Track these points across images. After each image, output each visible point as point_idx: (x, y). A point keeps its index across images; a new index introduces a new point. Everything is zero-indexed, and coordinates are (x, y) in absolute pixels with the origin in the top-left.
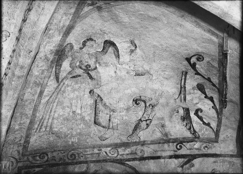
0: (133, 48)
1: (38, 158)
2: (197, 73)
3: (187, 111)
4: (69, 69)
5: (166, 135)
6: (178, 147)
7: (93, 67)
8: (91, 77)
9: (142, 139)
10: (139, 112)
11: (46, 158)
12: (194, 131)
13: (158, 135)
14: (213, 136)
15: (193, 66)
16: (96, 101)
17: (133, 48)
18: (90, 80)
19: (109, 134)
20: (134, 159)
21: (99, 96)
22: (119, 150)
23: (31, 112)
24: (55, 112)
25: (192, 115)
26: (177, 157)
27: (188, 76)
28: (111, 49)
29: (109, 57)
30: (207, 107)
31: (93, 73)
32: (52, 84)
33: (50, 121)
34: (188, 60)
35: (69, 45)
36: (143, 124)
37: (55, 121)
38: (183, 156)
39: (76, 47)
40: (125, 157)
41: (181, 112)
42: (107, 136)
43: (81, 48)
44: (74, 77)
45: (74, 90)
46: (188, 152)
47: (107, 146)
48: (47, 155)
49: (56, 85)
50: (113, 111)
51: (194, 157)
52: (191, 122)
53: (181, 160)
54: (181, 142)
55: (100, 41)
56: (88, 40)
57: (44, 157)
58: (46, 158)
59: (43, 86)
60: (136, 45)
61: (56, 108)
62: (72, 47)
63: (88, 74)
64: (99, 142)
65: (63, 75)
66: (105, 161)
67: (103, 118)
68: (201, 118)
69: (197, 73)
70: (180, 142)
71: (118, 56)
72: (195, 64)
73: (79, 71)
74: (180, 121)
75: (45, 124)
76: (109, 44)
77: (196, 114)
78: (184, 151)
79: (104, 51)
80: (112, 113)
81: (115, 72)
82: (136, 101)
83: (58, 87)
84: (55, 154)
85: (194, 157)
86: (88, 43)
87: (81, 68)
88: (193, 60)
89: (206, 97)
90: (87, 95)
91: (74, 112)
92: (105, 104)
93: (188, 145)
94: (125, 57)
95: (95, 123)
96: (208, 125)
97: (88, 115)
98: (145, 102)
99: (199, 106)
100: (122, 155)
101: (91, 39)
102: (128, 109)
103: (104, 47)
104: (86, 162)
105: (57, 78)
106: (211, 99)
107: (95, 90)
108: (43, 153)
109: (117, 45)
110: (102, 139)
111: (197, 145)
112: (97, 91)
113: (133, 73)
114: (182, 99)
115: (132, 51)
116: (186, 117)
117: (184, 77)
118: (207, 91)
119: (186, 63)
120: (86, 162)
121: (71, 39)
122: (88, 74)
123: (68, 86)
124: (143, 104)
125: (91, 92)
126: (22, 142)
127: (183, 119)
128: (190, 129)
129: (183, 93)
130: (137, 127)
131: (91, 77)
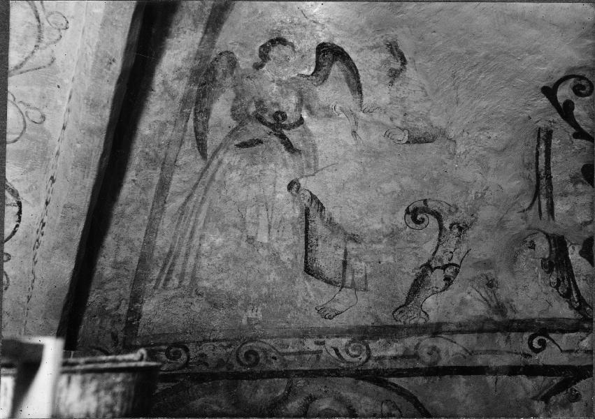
0: (397, 66)
1: (163, 356)
3: (559, 244)
5: (500, 309)
6: (535, 344)
7: (292, 117)
8: (289, 147)
9: (433, 318)
10: (427, 242)
11: (184, 356)
12: (581, 299)
13: (477, 308)
16: (307, 213)
17: (397, 66)
18: (287, 154)
19: (344, 300)
21: (313, 197)
22: (372, 345)
23: (141, 235)
24: (201, 237)
26: (531, 371)
27: (555, 143)
28: (337, 69)
29: (332, 92)
31: (293, 136)
32: (188, 157)
33: (191, 260)
34: (549, 92)
35: (224, 58)
36: (437, 278)
37: (204, 262)
38: (546, 370)
39: (246, 61)
40: (388, 364)
41: (543, 247)
42: (339, 307)
43: (258, 67)
44: (243, 145)
46: (564, 360)
47: (340, 334)
48: (187, 350)
49: (199, 166)
50: (353, 238)
52: (571, 276)
54: (544, 331)
56: (273, 42)
57: (177, 355)
58: (184, 356)
59: (167, 166)
60: (402, 58)
61: (204, 227)
62: (233, 64)
63: (282, 137)
64: (320, 323)
66: (336, 373)
67: (328, 257)
70: (543, 329)
71: (357, 89)
73: (259, 131)
75: (178, 268)
78: (552, 356)
80: (351, 245)
81: (354, 133)
82: (415, 214)
83: (205, 170)
86: (274, 52)
87: (260, 120)
88: (564, 93)
90: (282, 194)
92: (331, 221)
93: (564, 340)
95: (309, 270)
97: (288, 245)
98: (438, 216)
100: (380, 359)
101: (281, 41)
103: (317, 62)
104: (285, 374)
105: (201, 146)
107: (302, 181)
108: (177, 344)
109: (353, 56)
110: (323, 312)
113: (403, 137)
114: (544, 209)
115: (394, 75)
117: (542, 147)
119: (544, 102)
120: (285, 374)
121: (227, 39)
122: (282, 137)
123: (231, 168)
124: (432, 222)
126: (124, 310)
127: (548, 266)
128: (567, 295)
129: (543, 191)
130: (418, 285)
131: (289, 147)
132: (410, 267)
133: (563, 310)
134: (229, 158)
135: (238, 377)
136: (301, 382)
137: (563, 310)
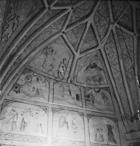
2: (64, 63)
4: (45, 51)
8: (46, 55)
9: (50, 74)
14: (62, 78)
15: (64, 61)
16: (44, 61)
20: (47, 77)
25: (59, 73)
26: (55, 80)
29: (51, 53)
30: (62, 71)
31: (47, 55)
34: (63, 59)
36: (51, 71)
38: (56, 80)
39: (48, 48)
41: (58, 71)
45: (43, 56)
46: (57, 80)
47: (43, 72)
50: (47, 65)
51: (59, 81)
53: (56, 81)
55: (52, 49)
62: (47, 48)
65: (43, 52)
66: (42, 75)
67: (44, 66)
68: (61, 74)
69: (64, 63)
70: (56, 78)
71: (52, 54)
72: (64, 61)
74: (57, 73)
76: (53, 50)
77: (60, 73)
78: (56, 79)
79: (51, 51)
84: (33, 69)
85: (59, 81)
88: (64, 60)
89: (63, 70)
91: (40, 61)
93: (58, 79)
94: (53, 55)
95: (42, 66)
96: (62, 76)
97: (42, 64)
99: (61, 71)
101: (51, 48)
102: (49, 66)
105: (42, 52)
106: (64, 70)
109: (54, 51)
111: (59, 79)
112: (46, 59)
115: (55, 54)
116: (58, 73)
118: (64, 68)
119: (63, 60)
121: (49, 46)
125: (45, 58)
130: (49, 71)
131: (46, 55)
132: (49, 69)
133: (58, 77)
134: (43, 54)
135: (34, 72)
136: (39, 75)
137: (58, 77)
